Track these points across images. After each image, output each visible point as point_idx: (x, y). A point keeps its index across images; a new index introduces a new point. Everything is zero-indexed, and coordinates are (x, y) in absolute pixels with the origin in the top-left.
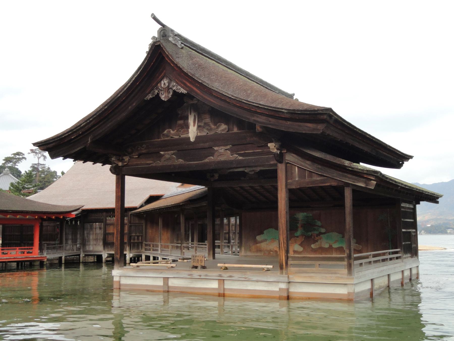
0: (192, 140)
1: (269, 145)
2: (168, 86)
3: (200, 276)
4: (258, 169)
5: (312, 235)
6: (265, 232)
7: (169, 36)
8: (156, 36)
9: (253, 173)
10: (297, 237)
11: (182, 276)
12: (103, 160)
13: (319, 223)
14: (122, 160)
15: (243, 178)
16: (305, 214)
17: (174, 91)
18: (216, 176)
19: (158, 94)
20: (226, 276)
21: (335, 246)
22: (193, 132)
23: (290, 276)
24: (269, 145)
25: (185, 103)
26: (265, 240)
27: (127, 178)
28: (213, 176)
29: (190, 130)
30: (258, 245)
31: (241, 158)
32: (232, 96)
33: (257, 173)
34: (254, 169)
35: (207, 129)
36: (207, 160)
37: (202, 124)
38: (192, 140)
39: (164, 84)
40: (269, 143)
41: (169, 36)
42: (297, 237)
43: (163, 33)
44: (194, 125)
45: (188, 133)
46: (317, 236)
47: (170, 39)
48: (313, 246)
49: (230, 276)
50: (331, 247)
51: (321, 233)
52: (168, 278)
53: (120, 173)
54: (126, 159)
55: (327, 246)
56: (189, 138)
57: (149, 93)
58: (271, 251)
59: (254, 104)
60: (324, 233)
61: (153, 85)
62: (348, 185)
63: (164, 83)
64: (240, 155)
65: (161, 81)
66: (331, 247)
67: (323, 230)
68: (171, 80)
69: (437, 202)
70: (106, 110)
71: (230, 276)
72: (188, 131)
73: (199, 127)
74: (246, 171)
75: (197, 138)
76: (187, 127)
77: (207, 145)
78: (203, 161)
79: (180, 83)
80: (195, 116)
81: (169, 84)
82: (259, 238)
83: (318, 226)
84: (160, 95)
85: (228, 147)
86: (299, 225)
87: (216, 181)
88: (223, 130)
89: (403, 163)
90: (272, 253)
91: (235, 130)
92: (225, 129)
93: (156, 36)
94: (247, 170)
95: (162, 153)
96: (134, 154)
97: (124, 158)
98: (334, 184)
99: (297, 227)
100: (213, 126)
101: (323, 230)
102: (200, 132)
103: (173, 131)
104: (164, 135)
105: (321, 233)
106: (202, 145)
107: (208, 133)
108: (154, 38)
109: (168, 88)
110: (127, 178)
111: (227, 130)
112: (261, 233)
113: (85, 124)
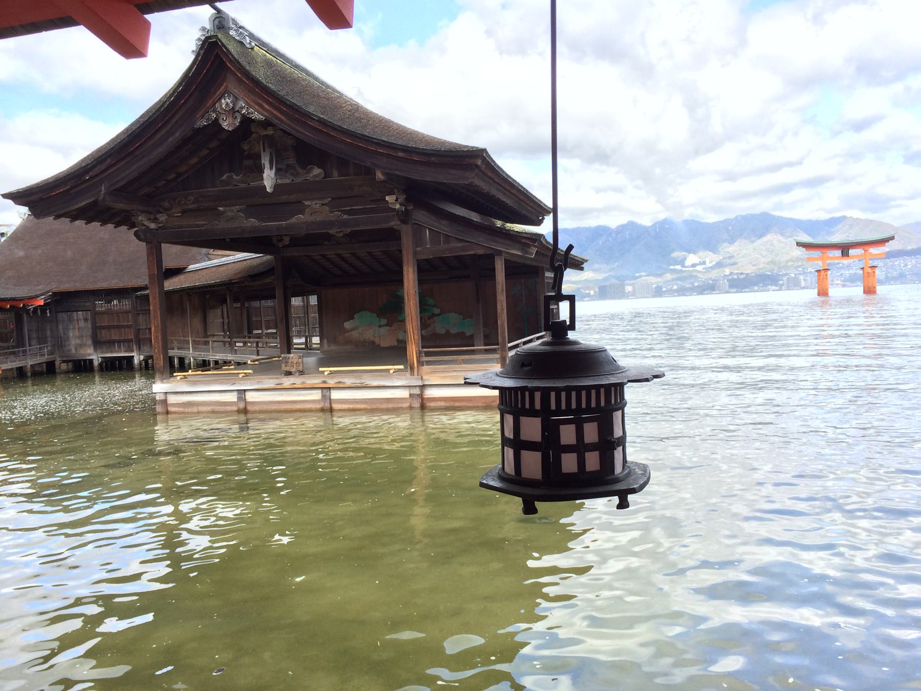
1: (387, 198)
2: (233, 108)
6: (355, 316)
7: (230, 28)
8: (208, 26)
9: (341, 235)
12: (123, 219)
14: (155, 220)
15: (326, 243)
18: (287, 240)
21: (454, 331)
22: (269, 179)
23: (425, 377)
24: (387, 198)
27: (164, 246)
28: (281, 240)
29: (265, 175)
31: (345, 217)
35: (292, 174)
36: (293, 220)
37: (284, 167)
39: (227, 104)
41: (230, 28)
44: (271, 169)
45: (263, 179)
46: (429, 319)
47: (232, 33)
50: (448, 332)
51: (434, 315)
52: (245, 390)
53: (153, 242)
54: (162, 218)
55: (443, 331)
62: (499, 253)
64: (345, 212)
65: (220, 99)
66: (448, 332)
67: (437, 311)
69: (582, 269)
73: (278, 171)
75: (276, 187)
77: (293, 197)
78: (288, 222)
79: (252, 104)
80: (271, 154)
81: (234, 103)
82: (347, 325)
84: (221, 121)
85: (326, 201)
87: (285, 246)
88: (316, 176)
89: (543, 219)
91: (335, 174)
93: (208, 26)
96: (174, 211)
97: (158, 216)
98: (481, 252)
100: (300, 171)
101: (437, 311)
102: (281, 179)
105: (434, 315)
106: (284, 198)
109: (233, 111)
110: (164, 246)
111: (322, 176)
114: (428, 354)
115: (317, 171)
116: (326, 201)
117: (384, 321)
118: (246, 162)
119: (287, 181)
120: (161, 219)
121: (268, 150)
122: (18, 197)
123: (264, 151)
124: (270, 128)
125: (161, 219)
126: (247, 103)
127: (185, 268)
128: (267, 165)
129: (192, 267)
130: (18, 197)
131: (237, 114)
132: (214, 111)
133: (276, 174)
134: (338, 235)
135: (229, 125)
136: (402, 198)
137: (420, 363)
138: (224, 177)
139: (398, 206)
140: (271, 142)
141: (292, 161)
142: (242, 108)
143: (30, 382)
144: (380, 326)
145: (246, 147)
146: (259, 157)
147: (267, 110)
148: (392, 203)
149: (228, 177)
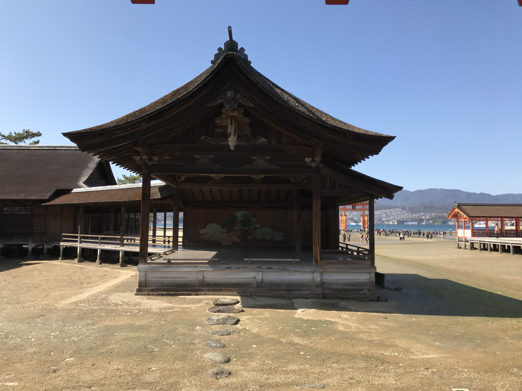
0: (232, 148)
1: (306, 159)
4: (223, 175)
6: (208, 226)
9: (219, 178)
13: (254, 220)
14: (150, 159)
16: (244, 212)
18: (183, 178)
22: (232, 142)
24: (306, 159)
29: (230, 139)
38: (232, 148)
42: (236, 231)
44: (235, 136)
48: (249, 238)
51: (256, 228)
54: (156, 158)
60: (259, 228)
73: (238, 137)
75: (236, 147)
76: (226, 136)
80: (235, 127)
82: (202, 231)
87: (181, 182)
91: (274, 142)
94: (212, 175)
95: (197, 156)
108: (220, 49)
115: (262, 140)
117: (225, 230)
118: (217, 130)
120: (155, 159)
121: (234, 124)
123: (231, 125)
124: (235, 112)
125: (155, 159)
128: (233, 133)
129: (75, 190)
131: (236, 101)
133: (237, 139)
136: (318, 159)
137: (321, 258)
138: (202, 138)
139: (314, 165)
141: (248, 132)
143: (76, 260)
144: (222, 233)
145: (218, 121)
146: (226, 127)
148: (309, 162)
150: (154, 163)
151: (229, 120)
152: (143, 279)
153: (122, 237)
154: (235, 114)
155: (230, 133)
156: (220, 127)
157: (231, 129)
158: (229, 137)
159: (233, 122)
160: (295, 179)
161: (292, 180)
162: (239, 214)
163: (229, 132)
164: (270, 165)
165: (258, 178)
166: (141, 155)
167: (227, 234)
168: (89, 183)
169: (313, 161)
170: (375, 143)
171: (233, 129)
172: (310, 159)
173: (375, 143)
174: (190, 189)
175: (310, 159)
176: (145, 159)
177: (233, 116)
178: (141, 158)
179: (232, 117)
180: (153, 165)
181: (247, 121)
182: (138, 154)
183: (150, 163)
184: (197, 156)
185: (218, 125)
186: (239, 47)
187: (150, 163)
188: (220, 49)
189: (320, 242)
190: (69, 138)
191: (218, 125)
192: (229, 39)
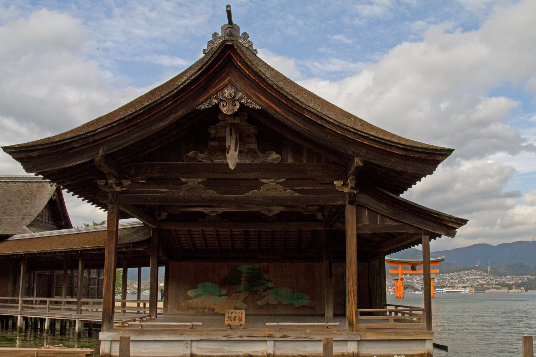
1: (336, 183)
2: (234, 97)
3: (241, 337)
4: (222, 210)
5: (258, 290)
6: (199, 286)
9: (214, 214)
10: (240, 292)
11: (214, 338)
14: (119, 184)
16: (251, 266)
17: (242, 105)
18: (164, 215)
19: (217, 105)
20: (278, 336)
21: (284, 303)
22: (232, 159)
24: (336, 183)
25: (220, 121)
26: (197, 296)
29: (228, 156)
30: (190, 301)
31: (297, 195)
32: (335, 121)
33: (219, 214)
34: (217, 209)
35: (252, 157)
36: (250, 193)
37: (245, 150)
38: (232, 167)
40: (336, 180)
43: (230, 31)
44: (235, 150)
46: (264, 291)
48: (258, 303)
49: (285, 336)
50: (280, 303)
52: (192, 341)
54: (127, 183)
56: (227, 165)
57: (205, 101)
58: (205, 308)
59: (363, 134)
61: (211, 92)
63: (228, 92)
66: (280, 303)
67: (271, 285)
68: (237, 90)
70: (139, 115)
71: (285, 336)
72: (225, 156)
73: (240, 152)
74: (205, 211)
75: (238, 165)
76: (224, 150)
77: (252, 176)
78: (246, 195)
80: (236, 138)
83: (265, 280)
84: (221, 107)
85: (281, 180)
86: (243, 279)
88: (274, 160)
90: (207, 311)
91: (290, 161)
92: (278, 158)
94: (206, 211)
95: (183, 180)
97: (123, 181)
99: (240, 281)
102: (241, 159)
103: (201, 153)
104: (187, 157)
105: (268, 288)
106: (244, 175)
107: (253, 161)
109: (233, 99)
112: (195, 287)
113: (103, 129)
114: (362, 314)
115: (274, 156)
116: (281, 180)
117: (224, 292)
118: (212, 143)
119: (248, 162)
120: (125, 184)
121: (234, 136)
122: (18, 152)
123: (231, 135)
125: (125, 184)
126: (247, 95)
127: (9, 236)
128: (233, 147)
130: (18, 152)
132: (216, 98)
134: (212, 214)
135: (228, 110)
136: (351, 183)
138: (191, 154)
139: (346, 190)
140: (236, 129)
141: (254, 146)
142: (241, 98)
144: (220, 296)
145: (212, 131)
146: (224, 139)
147: (264, 102)
148: (339, 187)
149: (194, 153)
150: (124, 189)
151: (228, 129)
152: (100, 270)
153: (78, 300)
154: (237, 122)
155: (229, 147)
156: (215, 139)
157: (231, 143)
158: (228, 153)
159: (233, 132)
160: (324, 215)
161: (319, 216)
162: (244, 268)
163: (227, 146)
164: (285, 190)
165: (271, 214)
166: (106, 179)
167: (228, 297)
168: (35, 225)
169: (345, 184)
170: (428, 158)
171: (233, 142)
172: (341, 182)
173: (428, 158)
174: (175, 230)
175: (341, 182)
176: (112, 183)
177: (234, 124)
178: (107, 183)
179: (232, 125)
180: (122, 192)
181: (253, 130)
182: (103, 176)
183: (118, 189)
184: (183, 180)
185: (212, 136)
186: (241, 32)
187: (118, 189)
188: (215, 35)
189: (356, 298)
190: (10, 153)
191: (212, 136)
192: (227, 22)
